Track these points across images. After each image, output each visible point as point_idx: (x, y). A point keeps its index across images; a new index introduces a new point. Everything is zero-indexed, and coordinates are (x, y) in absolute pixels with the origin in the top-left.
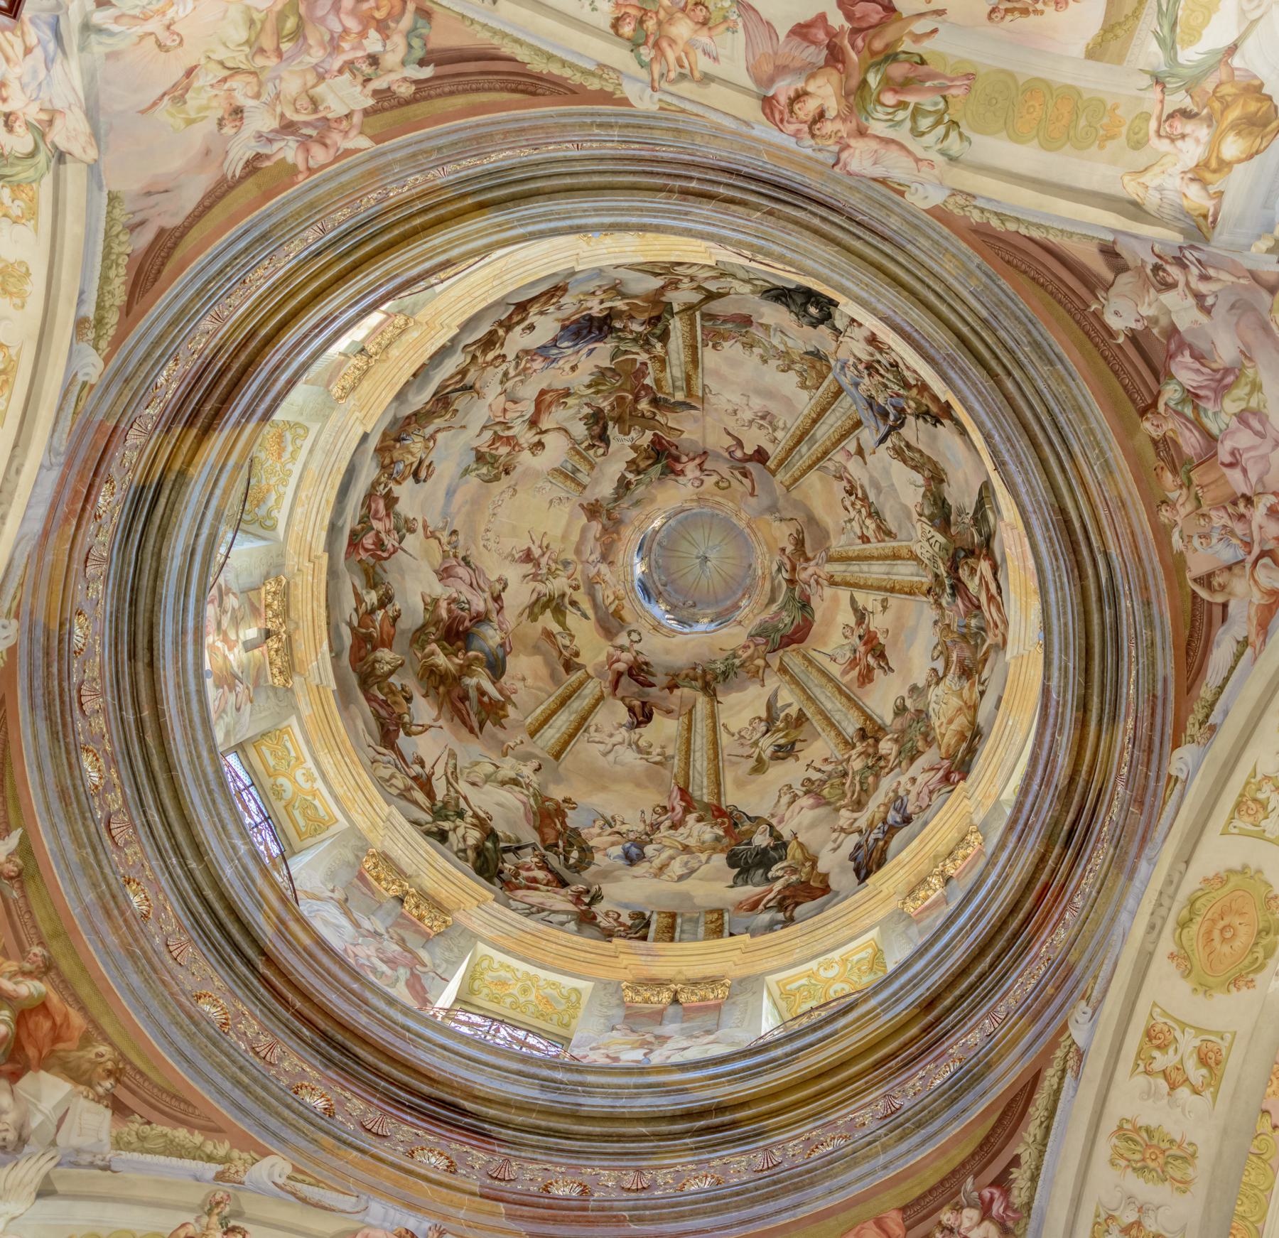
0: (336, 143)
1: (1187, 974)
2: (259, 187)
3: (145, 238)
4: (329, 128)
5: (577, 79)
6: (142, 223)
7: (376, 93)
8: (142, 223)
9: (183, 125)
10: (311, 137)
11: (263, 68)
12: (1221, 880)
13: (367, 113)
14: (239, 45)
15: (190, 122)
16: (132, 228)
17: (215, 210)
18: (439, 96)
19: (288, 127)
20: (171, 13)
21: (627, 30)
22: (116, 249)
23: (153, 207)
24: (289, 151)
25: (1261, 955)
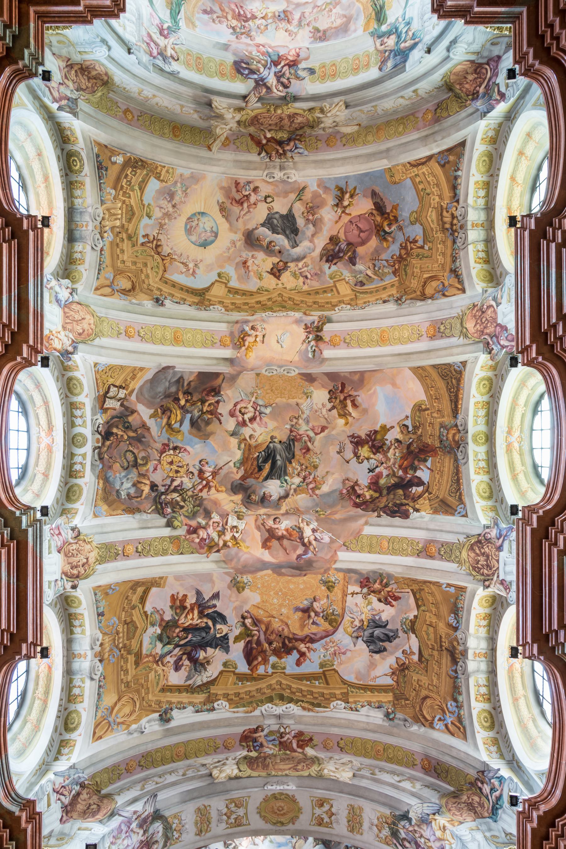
1: (297, 817)
12: (264, 818)
25: (283, 797)
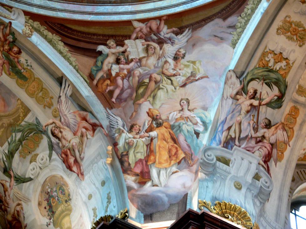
0: (146, 27)
2: (182, 21)
3: (232, 20)
4: (146, 35)
5: (42, 29)
6: (230, 27)
7: (122, 45)
8: (230, 27)
9: (197, 62)
10: (154, 34)
11: (158, 74)
13: (129, 37)
14: (162, 89)
15: (194, 63)
16: (233, 27)
17: (201, 18)
18: (100, 35)
19: (161, 42)
20: (179, 115)
21: (16, 49)
22: (243, 21)
23: (223, 32)
24: (165, 32)
